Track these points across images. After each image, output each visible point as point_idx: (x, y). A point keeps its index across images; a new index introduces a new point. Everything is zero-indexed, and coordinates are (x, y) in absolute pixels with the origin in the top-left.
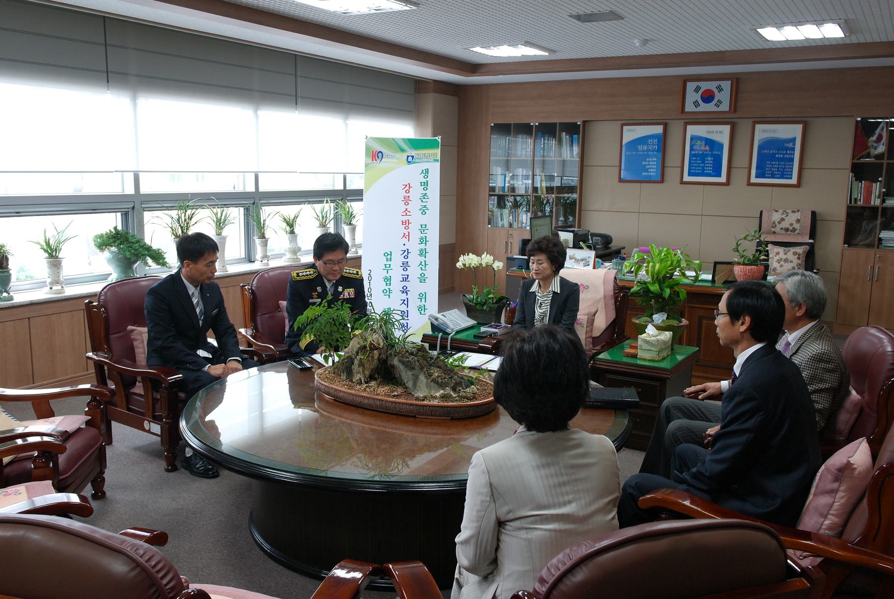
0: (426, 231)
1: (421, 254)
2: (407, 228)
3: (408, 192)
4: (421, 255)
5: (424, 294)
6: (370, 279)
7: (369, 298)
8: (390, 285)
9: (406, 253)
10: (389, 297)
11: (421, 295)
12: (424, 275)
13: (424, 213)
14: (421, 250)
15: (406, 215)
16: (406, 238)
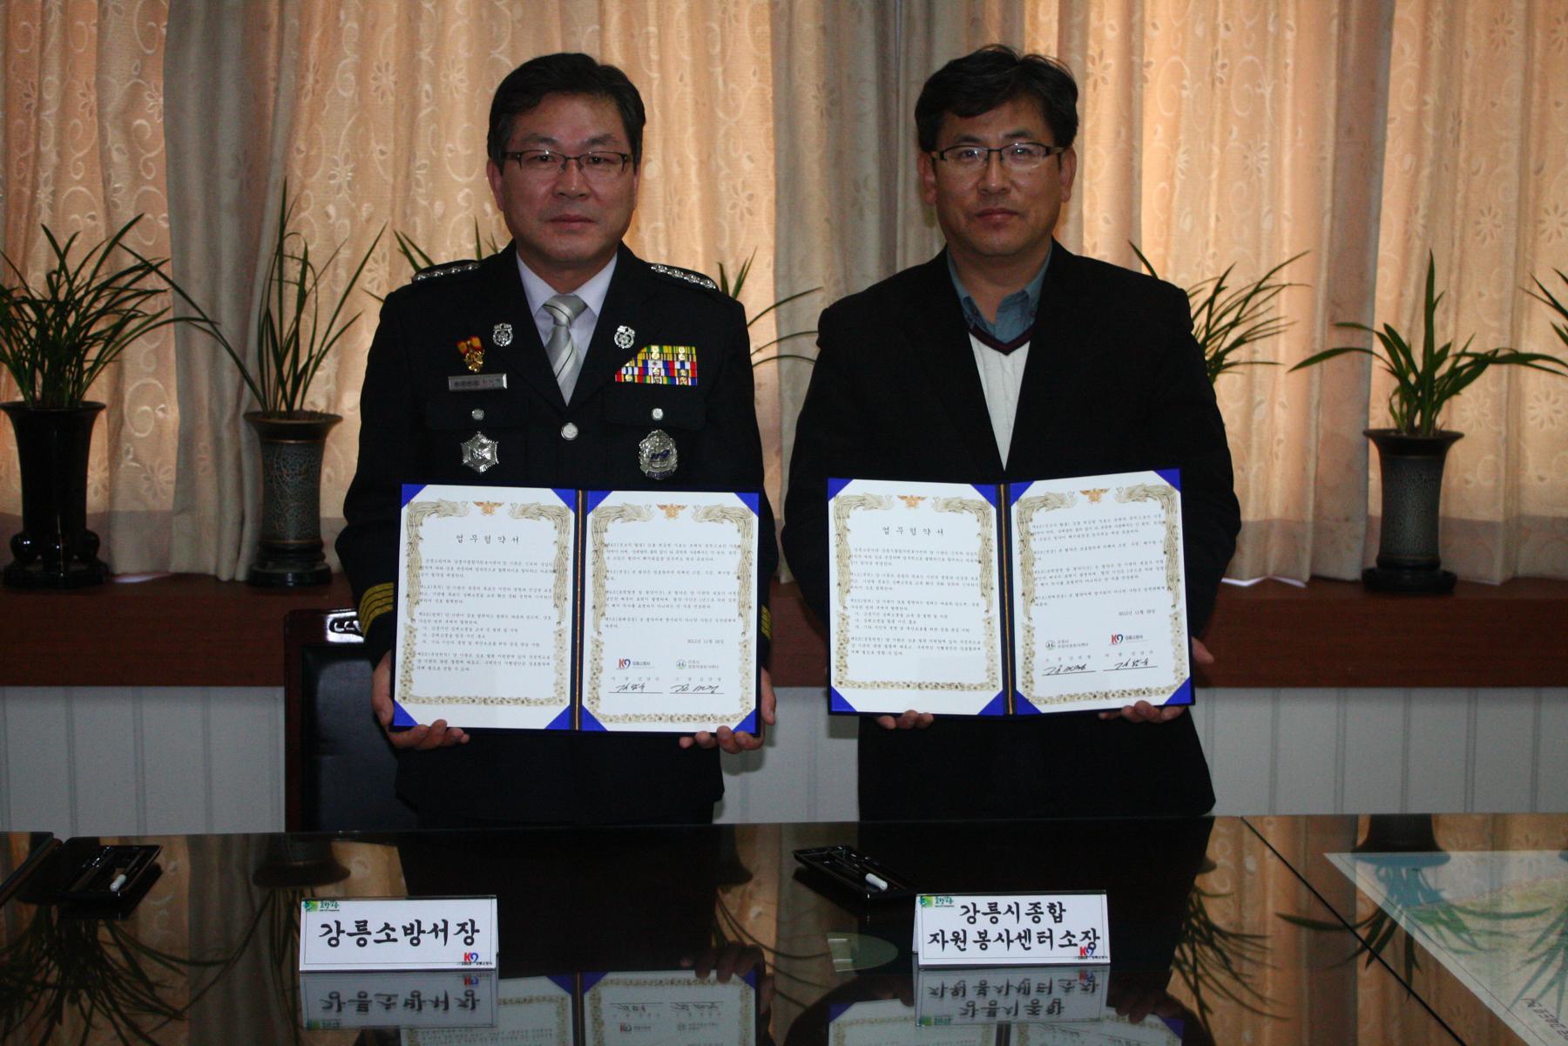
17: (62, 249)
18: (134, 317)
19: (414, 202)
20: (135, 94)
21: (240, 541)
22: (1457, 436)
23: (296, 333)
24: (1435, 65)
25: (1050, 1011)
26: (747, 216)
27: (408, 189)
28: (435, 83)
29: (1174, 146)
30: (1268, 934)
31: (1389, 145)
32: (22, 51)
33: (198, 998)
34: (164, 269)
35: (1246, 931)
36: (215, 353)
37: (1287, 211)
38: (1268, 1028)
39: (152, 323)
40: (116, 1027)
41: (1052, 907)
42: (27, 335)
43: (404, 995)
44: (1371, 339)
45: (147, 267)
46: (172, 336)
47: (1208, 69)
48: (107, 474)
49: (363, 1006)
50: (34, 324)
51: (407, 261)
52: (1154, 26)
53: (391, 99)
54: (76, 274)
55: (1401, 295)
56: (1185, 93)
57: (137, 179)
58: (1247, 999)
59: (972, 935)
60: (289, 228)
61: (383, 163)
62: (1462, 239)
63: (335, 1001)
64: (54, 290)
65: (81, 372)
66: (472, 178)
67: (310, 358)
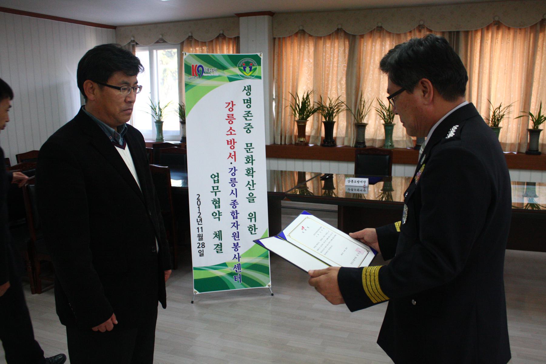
0: (251, 150)
1: (249, 173)
2: (232, 147)
3: (231, 110)
4: (248, 174)
6: (199, 204)
7: (200, 223)
8: (219, 208)
9: (234, 171)
10: (219, 220)
11: (251, 215)
12: (253, 195)
13: (248, 131)
14: (248, 170)
15: (231, 134)
16: (232, 158)
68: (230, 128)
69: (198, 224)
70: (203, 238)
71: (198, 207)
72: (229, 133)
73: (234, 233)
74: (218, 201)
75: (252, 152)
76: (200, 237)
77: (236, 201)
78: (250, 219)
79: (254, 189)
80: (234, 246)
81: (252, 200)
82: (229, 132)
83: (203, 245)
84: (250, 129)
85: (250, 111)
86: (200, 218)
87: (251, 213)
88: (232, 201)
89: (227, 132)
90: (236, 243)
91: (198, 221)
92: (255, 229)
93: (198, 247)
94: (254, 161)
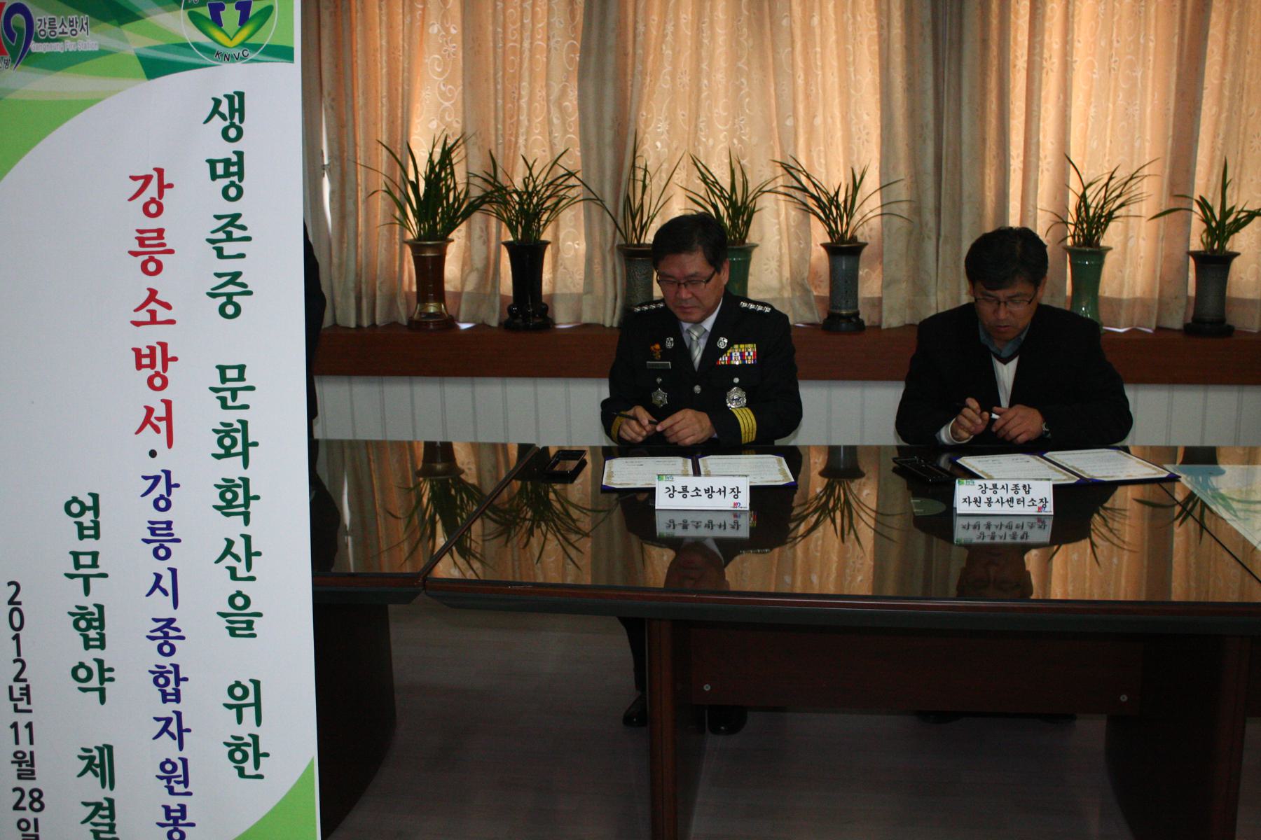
0: (243, 397)
1: (229, 504)
3: (154, 208)
4: (226, 508)
5: (251, 687)
6: (17, 623)
7: (22, 705)
8: (102, 646)
10: (103, 700)
11: (238, 692)
13: (230, 309)
14: (227, 487)
15: (153, 321)
16: (157, 430)
17: (530, 165)
18: (564, 198)
19: (699, 140)
20: (563, 92)
21: (615, 307)
22: (1237, 254)
23: (642, 205)
24: (1230, 59)
25: (1022, 538)
26: (865, 143)
27: (696, 133)
28: (709, 81)
29: (1088, 104)
30: (1128, 508)
31: (1204, 101)
32: (511, 71)
33: (596, 526)
34: (578, 175)
35: (1116, 507)
36: (602, 215)
37: (1148, 137)
38: (1126, 556)
39: (573, 201)
40: (559, 540)
41: (1024, 486)
42: (514, 208)
43: (705, 521)
44: (1192, 203)
45: (570, 174)
46: (582, 207)
47: (1107, 63)
48: (551, 275)
49: (685, 527)
50: (517, 203)
51: (696, 168)
52: (1079, 41)
53: (687, 88)
54: (537, 178)
55: (1208, 180)
56: (1095, 76)
57: (566, 132)
58: (1115, 541)
59: (984, 499)
60: (638, 154)
61: (683, 120)
62: (1243, 150)
63: (672, 524)
64: (527, 186)
65: (539, 226)
66: (727, 127)
67: (648, 218)
68: (148, 293)
69: (16, 710)
70: (36, 768)
71: (14, 638)
72: (144, 316)
73: (168, 761)
74: (97, 616)
75: (246, 407)
76: (24, 766)
77: (173, 625)
78: (234, 710)
79: (252, 579)
80: (168, 817)
81: (244, 625)
82: (144, 311)
83: (34, 800)
84: (235, 299)
85: (238, 216)
86: (23, 685)
87: (238, 684)
88: (156, 620)
89: (136, 310)
90: (174, 806)
91: (17, 694)
92: (257, 756)
93: (16, 807)
94: (251, 449)
